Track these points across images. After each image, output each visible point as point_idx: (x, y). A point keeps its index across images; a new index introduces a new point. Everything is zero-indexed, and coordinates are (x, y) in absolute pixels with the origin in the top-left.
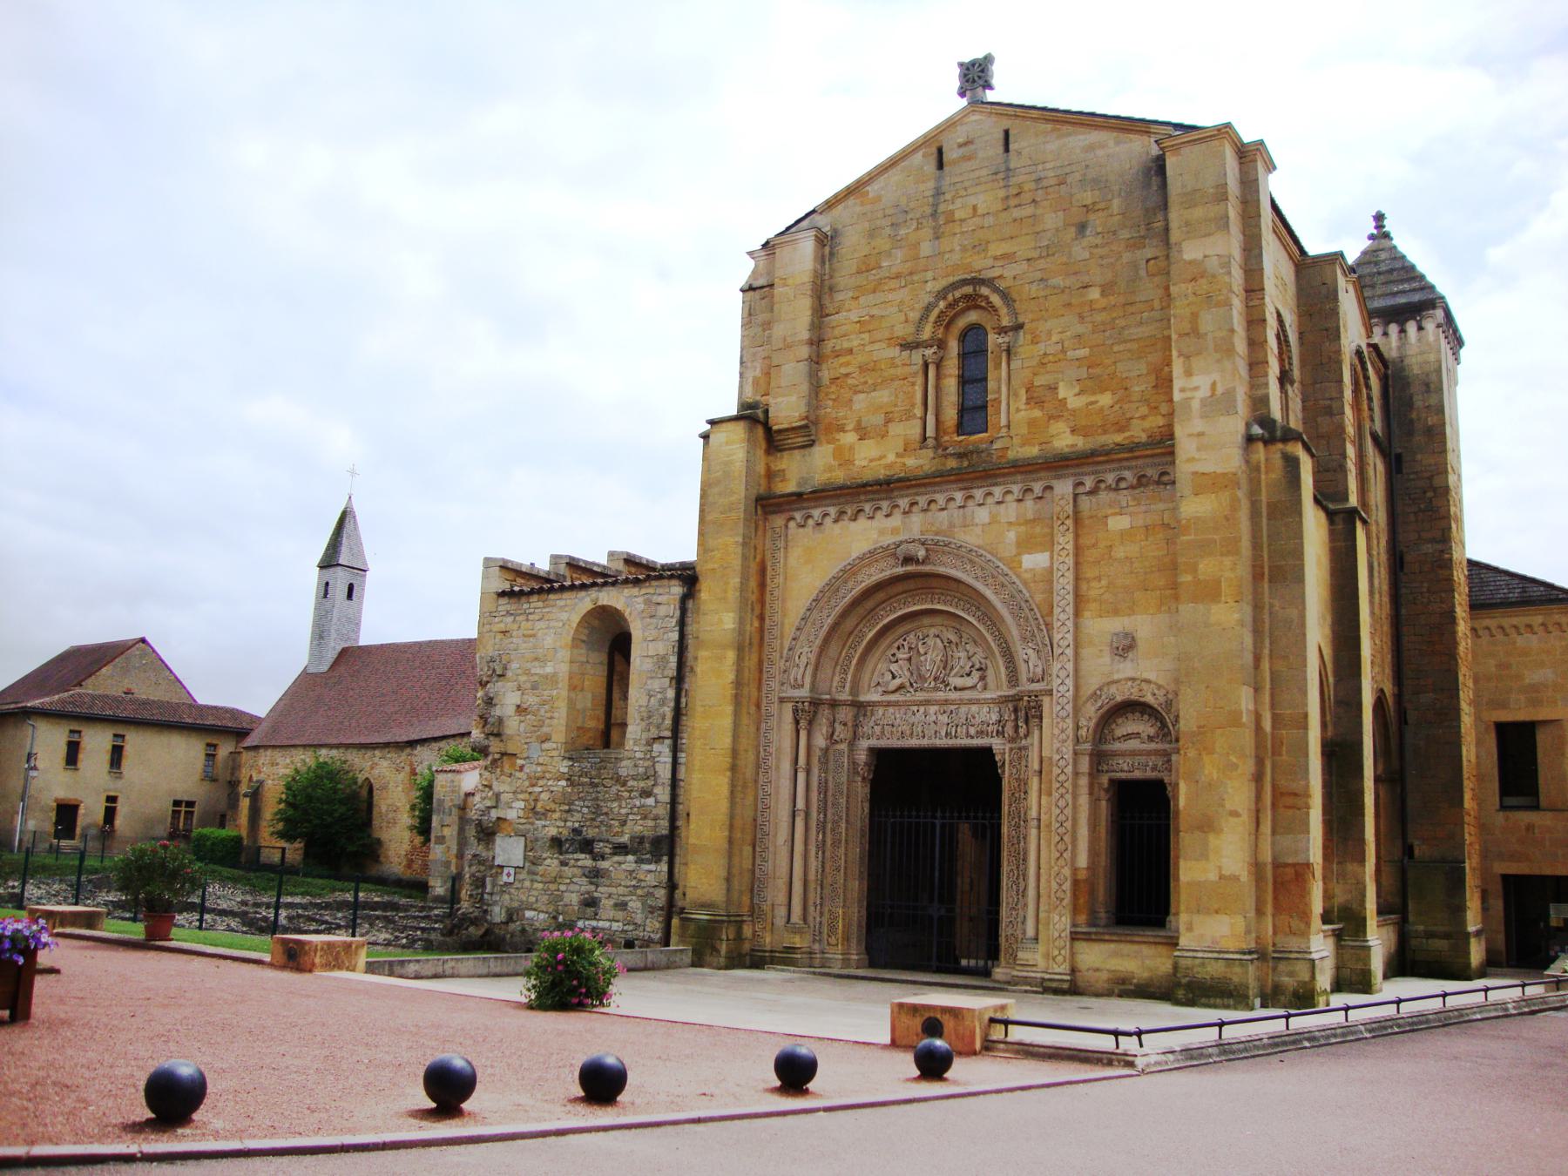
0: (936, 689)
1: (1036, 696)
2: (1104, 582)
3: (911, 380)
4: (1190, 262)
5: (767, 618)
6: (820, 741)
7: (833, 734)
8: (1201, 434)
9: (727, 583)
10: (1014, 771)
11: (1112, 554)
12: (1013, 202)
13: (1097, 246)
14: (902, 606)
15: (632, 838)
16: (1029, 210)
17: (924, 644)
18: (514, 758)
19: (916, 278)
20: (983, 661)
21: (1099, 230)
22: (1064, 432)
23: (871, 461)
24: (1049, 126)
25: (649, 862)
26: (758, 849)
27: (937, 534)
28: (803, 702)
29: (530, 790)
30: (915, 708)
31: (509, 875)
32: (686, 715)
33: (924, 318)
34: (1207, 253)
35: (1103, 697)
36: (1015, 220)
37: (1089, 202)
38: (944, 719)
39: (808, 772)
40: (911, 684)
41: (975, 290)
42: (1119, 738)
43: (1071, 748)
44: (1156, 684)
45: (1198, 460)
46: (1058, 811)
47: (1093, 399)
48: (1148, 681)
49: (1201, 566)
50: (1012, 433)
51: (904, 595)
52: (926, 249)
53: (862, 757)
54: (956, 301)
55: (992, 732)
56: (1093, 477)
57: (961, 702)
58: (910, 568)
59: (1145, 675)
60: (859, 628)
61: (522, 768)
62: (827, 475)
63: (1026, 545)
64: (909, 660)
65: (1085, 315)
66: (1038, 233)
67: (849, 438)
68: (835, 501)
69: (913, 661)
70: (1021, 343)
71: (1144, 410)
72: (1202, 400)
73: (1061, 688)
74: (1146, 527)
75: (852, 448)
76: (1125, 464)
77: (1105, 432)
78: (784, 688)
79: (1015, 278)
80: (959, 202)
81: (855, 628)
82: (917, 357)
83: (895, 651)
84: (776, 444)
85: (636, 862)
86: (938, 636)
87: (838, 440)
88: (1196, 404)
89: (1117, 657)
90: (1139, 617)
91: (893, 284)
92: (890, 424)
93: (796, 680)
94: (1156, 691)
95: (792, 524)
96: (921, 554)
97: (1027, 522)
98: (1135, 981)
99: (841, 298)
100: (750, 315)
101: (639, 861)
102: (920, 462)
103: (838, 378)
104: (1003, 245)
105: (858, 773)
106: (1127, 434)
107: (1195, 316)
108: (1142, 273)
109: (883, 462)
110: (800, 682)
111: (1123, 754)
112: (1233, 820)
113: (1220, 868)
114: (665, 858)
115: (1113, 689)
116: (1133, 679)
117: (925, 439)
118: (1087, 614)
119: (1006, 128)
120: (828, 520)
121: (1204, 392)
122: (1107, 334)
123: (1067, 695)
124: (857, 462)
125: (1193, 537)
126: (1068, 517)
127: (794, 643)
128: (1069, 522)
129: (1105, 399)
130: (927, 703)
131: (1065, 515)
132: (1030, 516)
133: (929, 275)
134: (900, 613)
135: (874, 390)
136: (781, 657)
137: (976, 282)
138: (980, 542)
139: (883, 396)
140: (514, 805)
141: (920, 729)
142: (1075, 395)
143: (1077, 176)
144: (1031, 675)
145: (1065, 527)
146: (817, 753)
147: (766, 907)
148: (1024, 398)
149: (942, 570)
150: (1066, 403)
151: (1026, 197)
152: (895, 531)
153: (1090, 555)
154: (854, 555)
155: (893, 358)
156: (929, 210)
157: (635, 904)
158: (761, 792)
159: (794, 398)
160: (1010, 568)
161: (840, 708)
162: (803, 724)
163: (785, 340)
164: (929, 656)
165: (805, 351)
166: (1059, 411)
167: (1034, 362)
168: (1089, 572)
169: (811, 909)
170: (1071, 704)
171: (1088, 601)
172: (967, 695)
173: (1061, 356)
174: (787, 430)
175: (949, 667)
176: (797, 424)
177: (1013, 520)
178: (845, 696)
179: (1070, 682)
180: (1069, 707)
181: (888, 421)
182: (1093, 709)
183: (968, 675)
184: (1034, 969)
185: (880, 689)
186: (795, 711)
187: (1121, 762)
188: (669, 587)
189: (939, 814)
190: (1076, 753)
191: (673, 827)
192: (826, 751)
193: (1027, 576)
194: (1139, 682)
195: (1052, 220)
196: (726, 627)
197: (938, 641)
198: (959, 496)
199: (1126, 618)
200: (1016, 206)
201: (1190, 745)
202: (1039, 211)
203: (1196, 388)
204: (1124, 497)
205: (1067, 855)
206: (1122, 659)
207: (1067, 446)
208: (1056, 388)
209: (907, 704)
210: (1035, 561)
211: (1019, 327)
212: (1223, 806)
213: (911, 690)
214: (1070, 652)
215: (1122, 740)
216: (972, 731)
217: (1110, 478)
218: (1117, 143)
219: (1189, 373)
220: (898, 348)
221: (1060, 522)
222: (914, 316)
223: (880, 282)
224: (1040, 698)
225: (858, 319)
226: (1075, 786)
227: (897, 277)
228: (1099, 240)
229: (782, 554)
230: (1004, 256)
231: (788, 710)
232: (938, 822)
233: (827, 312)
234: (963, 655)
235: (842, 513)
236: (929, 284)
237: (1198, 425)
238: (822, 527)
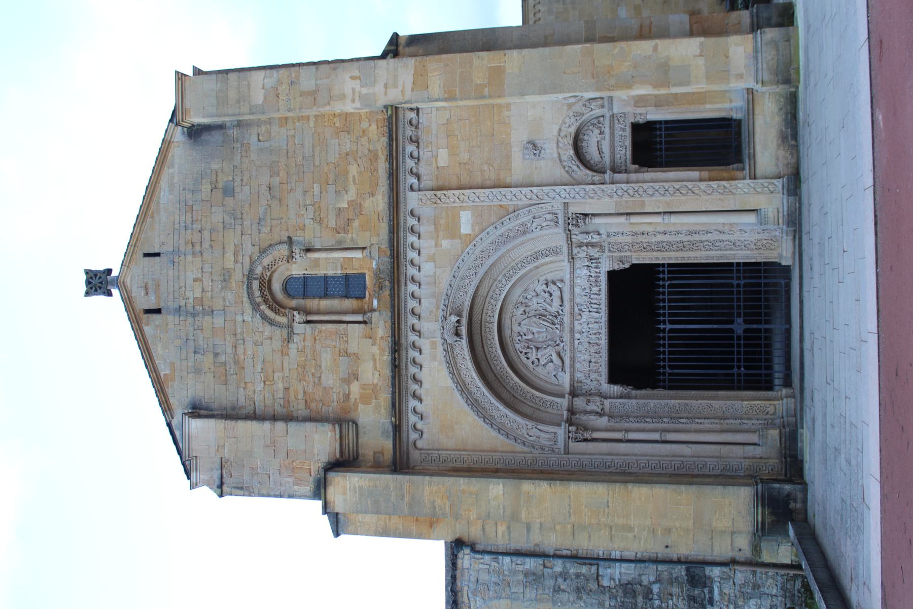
0: (562, 324)
1: (569, 219)
2: (486, 168)
3: (317, 333)
4: (265, 99)
5: (496, 467)
6: (603, 421)
7: (597, 413)
8: (386, 86)
9: (464, 492)
10: (626, 247)
11: (465, 162)
12: (198, 248)
13: (242, 180)
14: (494, 350)
16: (206, 234)
17: (525, 335)
19: (239, 330)
20: (540, 283)
21: (231, 178)
22: (373, 201)
23: (376, 369)
24: (149, 220)
25: (711, 592)
26: (696, 472)
27: (438, 307)
28: (569, 432)
30: (577, 342)
32: (577, 550)
33: (272, 323)
34: (261, 87)
35: (571, 165)
36: (211, 246)
37: (209, 187)
38: (585, 316)
39: (627, 431)
40: (557, 345)
41: (256, 279)
42: (601, 157)
43: (608, 186)
44: (561, 125)
45: (404, 87)
46: (657, 194)
47: (351, 179)
48: (560, 130)
49: (478, 82)
50: (367, 245)
51: (485, 348)
52: (219, 321)
53: (616, 389)
54: (263, 296)
55: (596, 272)
56: (407, 191)
57: (572, 300)
58: (464, 330)
59: (555, 133)
60: (510, 390)
62: (383, 411)
63: (453, 231)
64: (538, 348)
65: (289, 188)
66: (224, 227)
67: (355, 388)
68: (404, 399)
69: (539, 345)
70: (302, 239)
71: (364, 141)
72: (362, 86)
73: (563, 196)
74: (448, 136)
75: (363, 387)
76: (401, 149)
77: (376, 170)
78: (557, 451)
79: (254, 245)
80: (189, 294)
81: (509, 392)
82: (299, 328)
83: (530, 361)
84: (351, 459)
85: (712, 605)
86: (520, 324)
87: (356, 399)
88: (364, 91)
89: (542, 155)
90: (512, 140)
91: (240, 350)
92: (349, 351)
93: (550, 440)
94: (567, 125)
95: (420, 444)
96: (454, 318)
97: (436, 230)
98: (784, 129)
99: (243, 398)
100: (242, 488)
102: (381, 323)
103: (306, 401)
104: (227, 255)
105: (629, 393)
106: (380, 153)
107: (303, 94)
108: (267, 144)
109: (377, 357)
110: (551, 436)
111: (613, 154)
112: (660, 49)
113: (695, 56)
114: (708, 570)
115: (564, 158)
116: (558, 142)
117: (365, 322)
118: (508, 180)
119: (142, 255)
120: (420, 407)
121: (356, 84)
122: (306, 170)
123: (568, 190)
124: (376, 381)
125: (457, 89)
126: (435, 195)
127: (519, 441)
128: (439, 193)
129: (353, 170)
130: (572, 331)
131: (434, 197)
132: (431, 228)
133: (239, 318)
134: (499, 352)
135: (320, 366)
136: (531, 453)
137: (250, 276)
138: (449, 268)
139: (326, 358)
141: (593, 337)
142: (347, 193)
143: (189, 196)
144: (552, 223)
145: (443, 197)
146: (612, 424)
147: (746, 463)
148: (342, 235)
149: (467, 304)
150: (352, 201)
151: (196, 238)
152: (433, 345)
153: (465, 180)
154: (449, 383)
155: (298, 348)
156: (190, 320)
158: (646, 470)
159: (316, 437)
160: (470, 244)
161: (575, 407)
162: (587, 435)
163: (267, 446)
164: (535, 330)
165: (280, 425)
166: (357, 206)
167: (317, 227)
168: (478, 180)
169: (745, 427)
170: (575, 187)
171: (499, 179)
172: (566, 296)
173: (317, 206)
174: (341, 445)
175: (545, 313)
176: (338, 432)
177: (433, 242)
178: (564, 402)
179: (558, 189)
180: (577, 188)
181: (347, 354)
182: (579, 172)
183: (551, 295)
184: (781, 210)
185: (560, 374)
186: (577, 440)
187: (619, 156)
188: (463, 569)
189: (662, 326)
190: (613, 183)
191: (679, 562)
192: (611, 417)
193: (477, 229)
194: (560, 139)
195: (218, 216)
196: (501, 492)
197: (523, 322)
198: (412, 287)
199: (513, 150)
200: (201, 246)
201: (606, 83)
202: (209, 227)
203: (353, 90)
204: (425, 154)
205: (690, 185)
206: (543, 152)
207: (383, 199)
208: (340, 208)
209: (573, 350)
211: (290, 241)
212: (650, 56)
213: (562, 345)
214: (535, 190)
215: (603, 155)
216: (595, 290)
217: (410, 163)
218: (172, 166)
219: (343, 97)
220: (291, 345)
221: (439, 201)
222: (268, 330)
223: (236, 362)
224: (570, 215)
225: (262, 383)
226: (637, 182)
227: (236, 347)
228: (238, 179)
229: (444, 452)
230: (236, 255)
231: (573, 445)
232: (669, 327)
233: (252, 412)
234: (535, 300)
235: (414, 396)
236: (245, 318)
237: (379, 89)
238: (424, 415)
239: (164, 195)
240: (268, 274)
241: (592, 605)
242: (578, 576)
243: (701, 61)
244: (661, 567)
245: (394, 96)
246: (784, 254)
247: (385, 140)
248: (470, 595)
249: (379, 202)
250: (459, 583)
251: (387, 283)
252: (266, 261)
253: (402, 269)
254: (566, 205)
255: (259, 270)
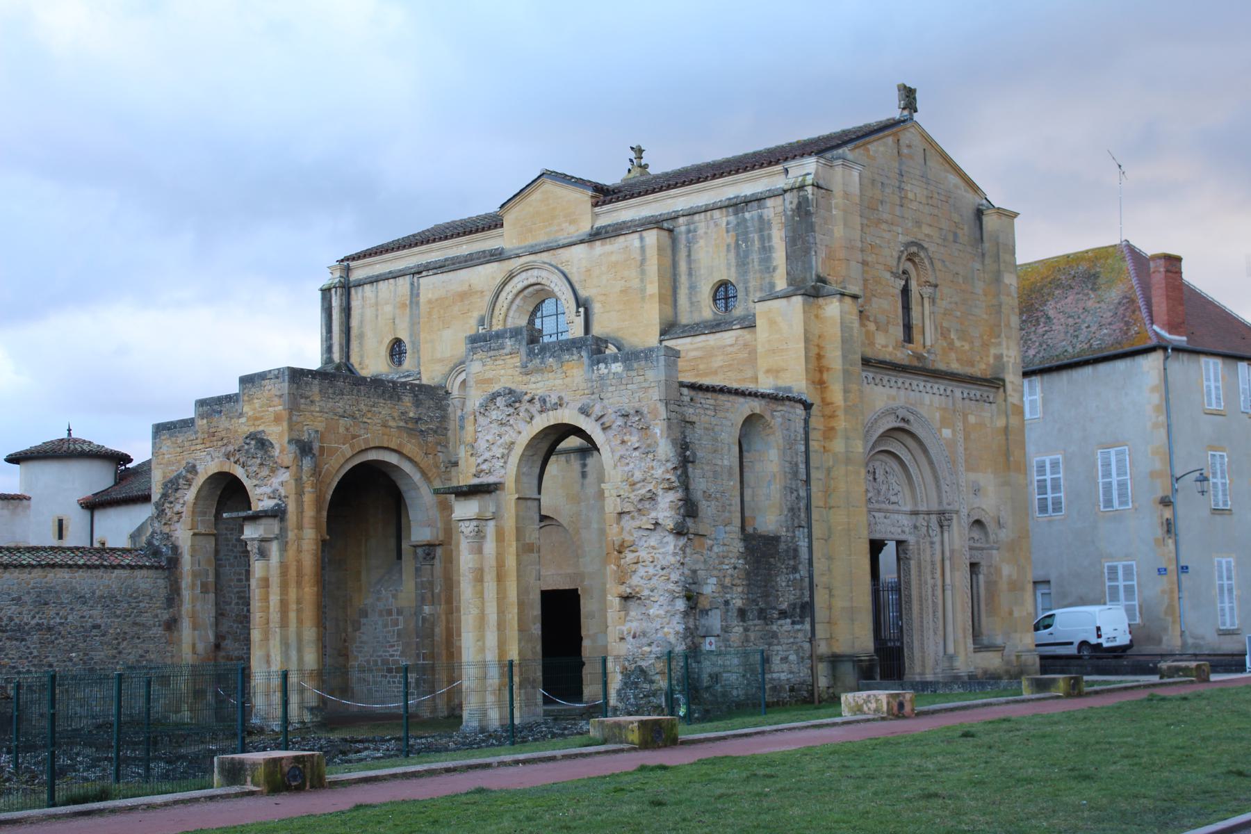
15: (789, 606)
16: (936, 211)
18: (702, 539)
24: (941, 160)
27: (911, 404)
29: (719, 567)
31: (711, 644)
48: (983, 510)
61: (710, 549)
63: (945, 423)
88: (1010, 365)
101: (793, 623)
102: (903, 356)
114: (808, 620)
121: (1012, 360)
140: (709, 581)
157: (793, 657)
172: (895, 507)
191: (812, 596)
202: (940, 215)
210: (947, 433)
211: (936, 286)
218: (966, 191)
222: (896, 254)
239: (953, 179)
240: (917, 261)
241: (787, 521)
242: (799, 509)
243: (1025, 614)
244: (807, 580)
245: (1009, 386)
246: (927, 676)
247: (979, 375)
248: (783, 412)
249: (955, 367)
250: (787, 403)
251: (920, 365)
252: (926, 261)
253: (932, 380)
254: (957, 512)
255: (922, 254)
